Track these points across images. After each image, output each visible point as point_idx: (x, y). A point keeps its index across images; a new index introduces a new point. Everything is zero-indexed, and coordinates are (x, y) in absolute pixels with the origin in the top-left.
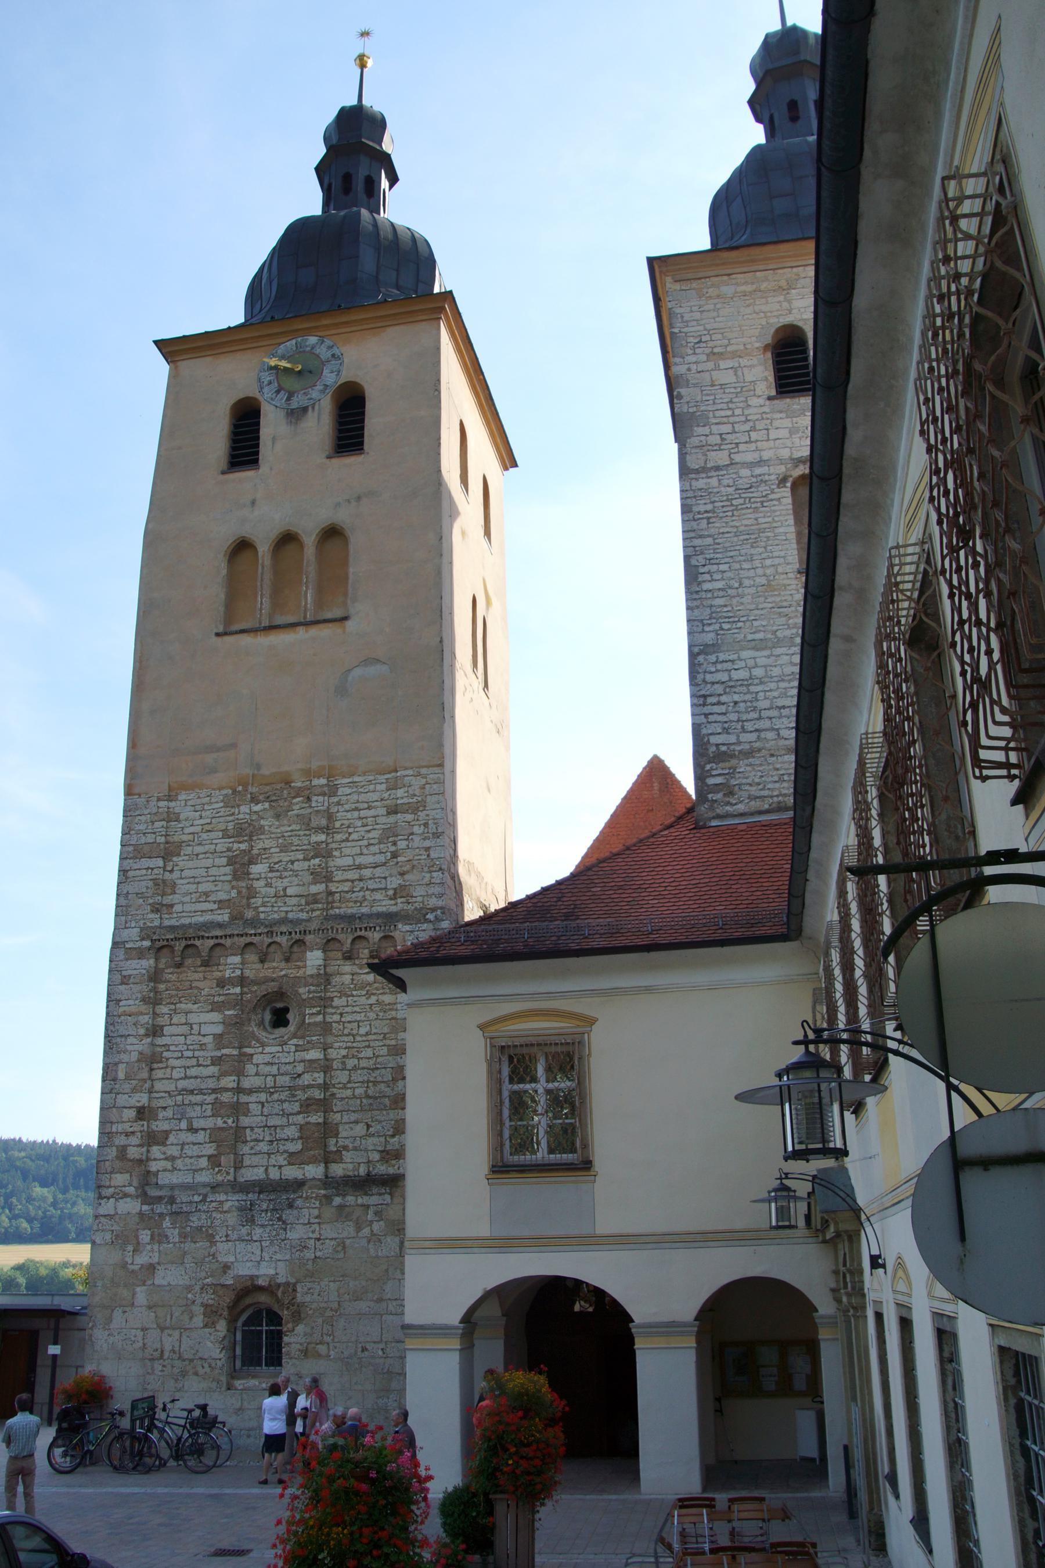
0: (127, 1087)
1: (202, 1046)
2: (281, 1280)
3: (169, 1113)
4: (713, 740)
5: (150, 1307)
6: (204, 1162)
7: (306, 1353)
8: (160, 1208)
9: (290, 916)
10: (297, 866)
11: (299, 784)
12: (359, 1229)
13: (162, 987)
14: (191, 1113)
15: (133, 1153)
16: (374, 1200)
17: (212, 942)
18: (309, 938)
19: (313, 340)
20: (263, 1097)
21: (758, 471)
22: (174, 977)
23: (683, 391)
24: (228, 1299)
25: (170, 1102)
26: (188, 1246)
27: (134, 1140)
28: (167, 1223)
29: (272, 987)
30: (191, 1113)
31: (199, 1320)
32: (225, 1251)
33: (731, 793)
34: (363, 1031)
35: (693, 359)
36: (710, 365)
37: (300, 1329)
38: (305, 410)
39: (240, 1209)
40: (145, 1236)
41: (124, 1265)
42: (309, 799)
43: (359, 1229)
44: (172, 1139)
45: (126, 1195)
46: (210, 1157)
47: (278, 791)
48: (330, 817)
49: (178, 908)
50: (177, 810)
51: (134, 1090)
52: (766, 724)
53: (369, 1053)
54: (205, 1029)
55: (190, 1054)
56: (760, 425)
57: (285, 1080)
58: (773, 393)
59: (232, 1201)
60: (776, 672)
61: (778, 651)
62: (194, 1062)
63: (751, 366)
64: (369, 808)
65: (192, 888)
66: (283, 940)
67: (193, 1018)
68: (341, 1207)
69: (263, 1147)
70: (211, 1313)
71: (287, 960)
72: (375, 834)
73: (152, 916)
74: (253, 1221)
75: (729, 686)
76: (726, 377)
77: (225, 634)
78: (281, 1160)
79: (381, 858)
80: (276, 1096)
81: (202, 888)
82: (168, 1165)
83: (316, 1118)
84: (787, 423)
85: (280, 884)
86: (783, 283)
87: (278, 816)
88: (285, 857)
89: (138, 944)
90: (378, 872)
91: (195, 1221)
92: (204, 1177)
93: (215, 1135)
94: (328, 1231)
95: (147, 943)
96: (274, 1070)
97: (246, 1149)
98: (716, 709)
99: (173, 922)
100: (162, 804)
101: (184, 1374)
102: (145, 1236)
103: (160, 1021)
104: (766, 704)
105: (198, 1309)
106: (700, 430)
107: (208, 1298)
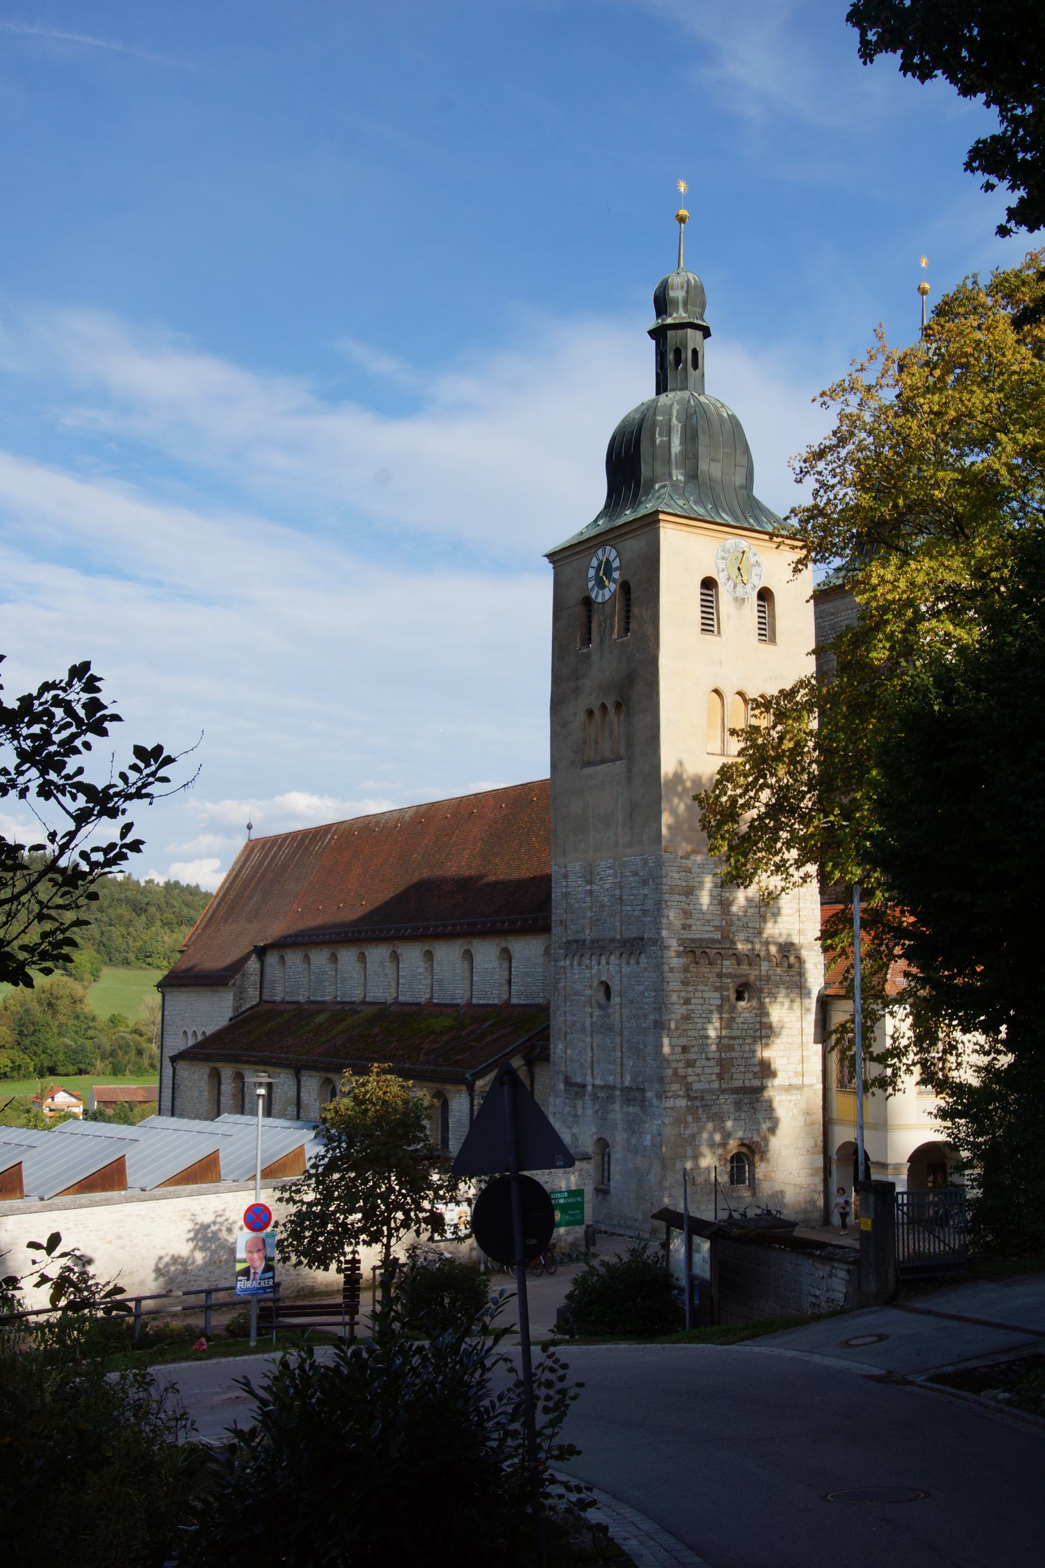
0: (676, 1034)
3: (696, 1049)
6: (714, 1077)
8: (697, 1103)
13: (689, 975)
15: (681, 1072)
16: (793, 1098)
17: (715, 951)
19: (744, 544)
20: (741, 1041)
22: (694, 970)
25: (695, 1043)
27: (681, 1065)
28: (700, 1111)
38: (743, 600)
39: (735, 1103)
40: (690, 1118)
41: (680, 1135)
44: (698, 1064)
45: (679, 1096)
46: (717, 1074)
49: (694, 928)
51: (680, 1036)
54: (712, 1002)
57: (750, 1032)
59: (731, 1098)
67: (706, 995)
71: (750, 965)
78: (750, 1076)
82: (697, 1079)
91: (714, 1110)
92: (716, 1085)
93: (720, 1062)
96: (746, 1026)
97: (734, 1070)
99: (692, 936)
100: (683, 861)
102: (690, 1118)
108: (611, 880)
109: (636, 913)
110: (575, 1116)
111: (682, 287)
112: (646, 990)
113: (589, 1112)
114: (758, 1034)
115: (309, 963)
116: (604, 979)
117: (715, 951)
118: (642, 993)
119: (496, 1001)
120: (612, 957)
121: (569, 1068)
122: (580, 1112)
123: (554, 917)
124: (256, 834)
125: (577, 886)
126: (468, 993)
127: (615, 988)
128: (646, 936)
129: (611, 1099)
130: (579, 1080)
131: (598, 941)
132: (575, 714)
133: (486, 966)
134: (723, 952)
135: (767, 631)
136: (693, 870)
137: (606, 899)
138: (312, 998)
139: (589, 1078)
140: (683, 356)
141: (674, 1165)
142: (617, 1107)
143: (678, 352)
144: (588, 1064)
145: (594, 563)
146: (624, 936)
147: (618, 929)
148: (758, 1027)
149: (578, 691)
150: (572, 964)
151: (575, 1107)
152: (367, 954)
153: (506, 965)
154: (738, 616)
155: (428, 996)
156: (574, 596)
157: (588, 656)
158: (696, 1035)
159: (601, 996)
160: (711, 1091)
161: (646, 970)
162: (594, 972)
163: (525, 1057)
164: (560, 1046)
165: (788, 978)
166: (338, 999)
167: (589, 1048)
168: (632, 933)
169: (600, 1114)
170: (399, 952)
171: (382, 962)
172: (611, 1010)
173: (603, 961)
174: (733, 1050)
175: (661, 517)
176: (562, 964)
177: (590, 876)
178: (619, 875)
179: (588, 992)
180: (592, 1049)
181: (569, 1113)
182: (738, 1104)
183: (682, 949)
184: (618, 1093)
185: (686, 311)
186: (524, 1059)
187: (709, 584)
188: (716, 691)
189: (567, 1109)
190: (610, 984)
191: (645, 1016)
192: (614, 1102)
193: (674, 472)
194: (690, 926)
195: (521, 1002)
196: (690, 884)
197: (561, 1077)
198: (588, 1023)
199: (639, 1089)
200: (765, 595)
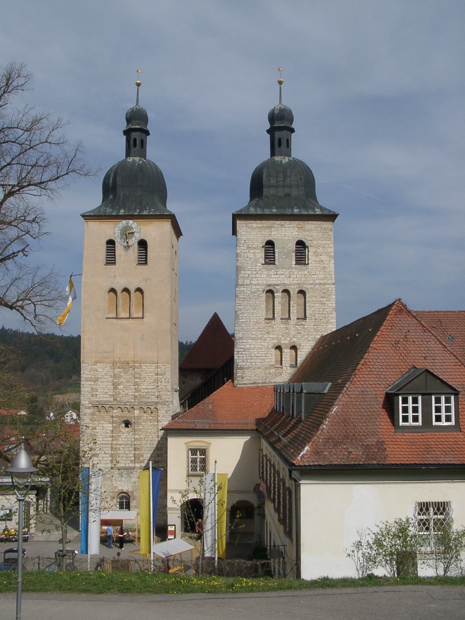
1: (107, 433)
4: (240, 364)
6: (109, 462)
10: (131, 387)
14: (105, 449)
18: (135, 407)
20: (124, 446)
21: (258, 287)
23: (239, 258)
24: (117, 494)
26: (106, 482)
30: (105, 449)
33: (243, 378)
35: (243, 248)
36: (247, 251)
37: (134, 502)
42: (134, 369)
44: (100, 456)
47: (126, 365)
48: (140, 375)
49: (98, 396)
52: (253, 361)
53: (151, 437)
56: (259, 272)
57: (130, 442)
58: (264, 263)
60: (256, 346)
61: (258, 341)
63: (258, 253)
65: (102, 391)
67: (104, 425)
69: (124, 458)
72: (152, 380)
74: (122, 476)
75: (245, 350)
76: (251, 256)
77: (109, 318)
78: (129, 462)
79: (154, 387)
83: (137, 452)
84: (266, 273)
85: (127, 392)
86: (270, 225)
87: (125, 373)
88: (128, 384)
90: (153, 390)
93: (112, 455)
95: (91, 405)
96: (126, 440)
98: (241, 355)
99: (98, 400)
103: (95, 426)
104: (253, 355)
106: (243, 272)
114: (133, 443)
148: (133, 440)
165: (151, 418)
174: (119, 450)
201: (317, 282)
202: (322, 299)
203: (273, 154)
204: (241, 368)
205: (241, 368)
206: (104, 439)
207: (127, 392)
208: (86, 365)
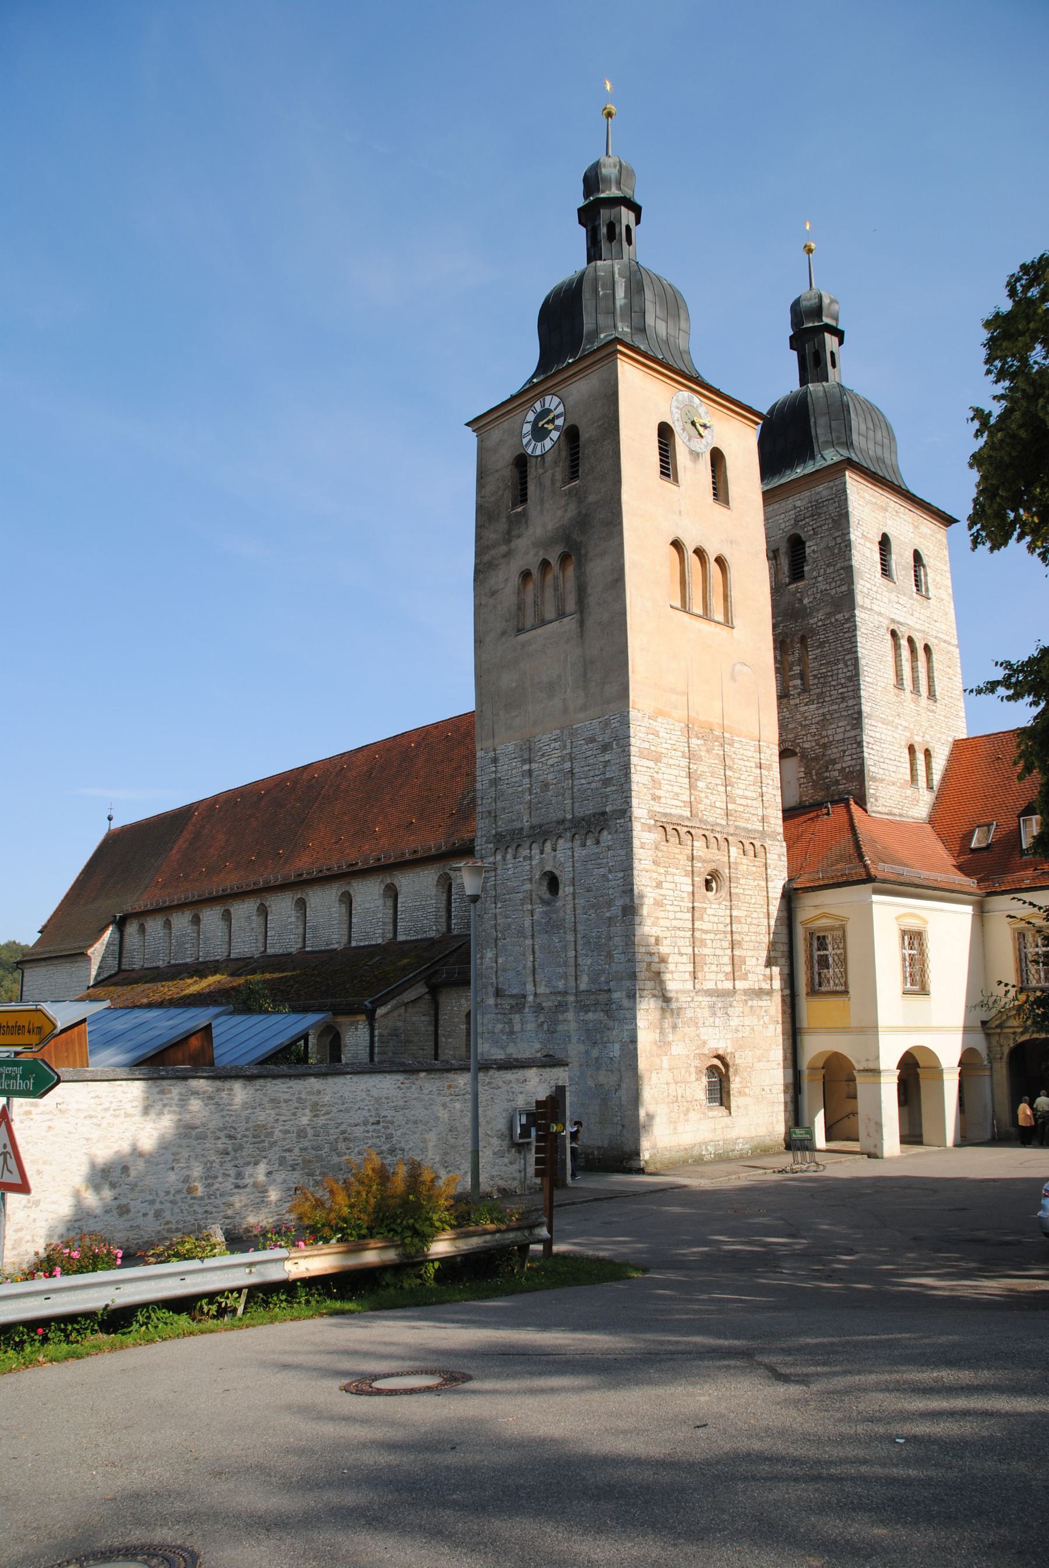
2: (729, 1051)
5: (670, 1069)
6: (687, 976)
7: (741, 1093)
9: (718, 821)
11: (716, 733)
12: (759, 1020)
13: (660, 854)
16: (764, 1003)
17: (686, 829)
18: (730, 838)
19: (696, 399)
20: (712, 936)
22: (665, 849)
25: (668, 934)
29: (713, 866)
31: (693, 1077)
32: (706, 1033)
34: (753, 901)
37: (737, 1079)
38: (698, 454)
39: (710, 1007)
43: (759, 1020)
47: (707, 733)
49: (663, 800)
50: (658, 729)
55: (676, 903)
57: (721, 927)
59: (705, 1000)
62: (678, 909)
64: (748, 761)
65: (670, 788)
66: (718, 836)
67: (677, 879)
68: (751, 1007)
70: (699, 1072)
73: (652, 802)
74: (714, 1014)
78: (721, 976)
80: (718, 937)
81: (677, 789)
85: (713, 798)
89: (648, 822)
94: (748, 1021)
96: (716, 919)
99: (661, 810)
100: (651, 721)
101: (688, 1110)
105: (693, 1070)
107: (697, 1063)
108: (558, 753)
109: (594, 785)
110: (512, 1032)
111: (615, 166)
112: (610, 871)
113: (530, 1026)
115: (170, 928)
116: (548, 868)
117: (686, 829)
118: (604, 876)
119: (380, 941)
120: (561, 841)
121: (501, 979)
122: (517, 1027)
123: (479, 809)
124: (116, 824)
125: (510, 768)
126: (346, 937)
127: (565, 876)
128: (608, 809)
129: (561, 1007)
130: (515, 992)
131: (540, 826)
132: (506, 580)
133: (367, 906)
134: (693, 831)
135: (720, 491)
136: (661, 735)
137: (551, 776)
138: (173, 962)
139: (530, 987)
140: (617, 231)
141: (650, 1078)
142: (570, 1016)
143: (611, 227)
144: (529, 971)
145: (531, 417)
146: (577, 814)
147: (569, 808)
149: (507, 555)
150: (504, 859)
151: (510, 1022)
152: (232, 910)
153: (390, 903)
154: (694, 472)
155: (300, 946)
156: (505, 456)
157: (524, 514)
158: (668, 925)
159: (544, 891)
160: (683, 992)
161: (609, 848)
162: (534, 862)
163: (427, 985)
164: (489, 954)
165: (754, 869)
166: (201, 960)
167: (529, 952)
168: (589, 808)
169: (545, 1027)
170: (267, 904)
171: (249, 917)
172: (559, 904)
173: (548, 846)
175: (619, 347)
176: (491, 859)
177: (528, 753)
178: (569, 745)
179: (528, 886)
180: (534, 952)
181: (502, 1031)
182: (712, 1007)
183: (652, 822)
184: (572, 998)
185: (620, 189)
186: (428, 986)
187: (665, 432)
188: (677, 544)
189: (500, 1026)
190: (557, 873)
191: (610, 903)
192: (566, 1011)
193: (619, 324)
194: (660, 798)
195: (409, 938)
196: (659, 750)
197: (491, 990)
198: (527, 923)
199: (601, 990)
200: (717, 458)
201: (941, 635)
202: (948, 670)
203: (803, 381)
204: (874, 779)
205: (874, 779)
206: (679, 915)
207: (713, 798)
208: (640, 715)
